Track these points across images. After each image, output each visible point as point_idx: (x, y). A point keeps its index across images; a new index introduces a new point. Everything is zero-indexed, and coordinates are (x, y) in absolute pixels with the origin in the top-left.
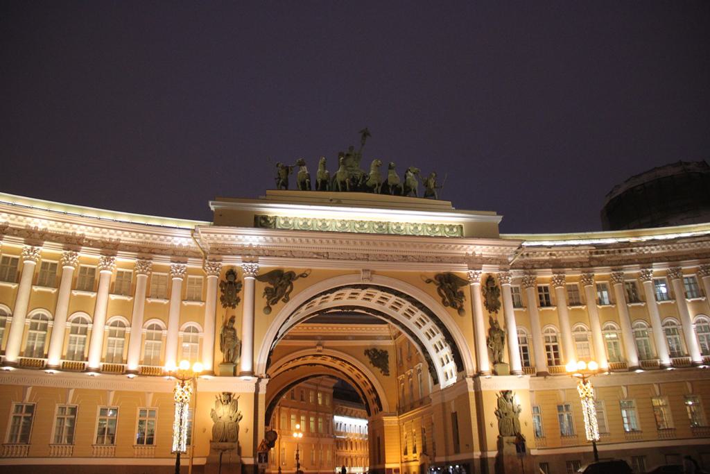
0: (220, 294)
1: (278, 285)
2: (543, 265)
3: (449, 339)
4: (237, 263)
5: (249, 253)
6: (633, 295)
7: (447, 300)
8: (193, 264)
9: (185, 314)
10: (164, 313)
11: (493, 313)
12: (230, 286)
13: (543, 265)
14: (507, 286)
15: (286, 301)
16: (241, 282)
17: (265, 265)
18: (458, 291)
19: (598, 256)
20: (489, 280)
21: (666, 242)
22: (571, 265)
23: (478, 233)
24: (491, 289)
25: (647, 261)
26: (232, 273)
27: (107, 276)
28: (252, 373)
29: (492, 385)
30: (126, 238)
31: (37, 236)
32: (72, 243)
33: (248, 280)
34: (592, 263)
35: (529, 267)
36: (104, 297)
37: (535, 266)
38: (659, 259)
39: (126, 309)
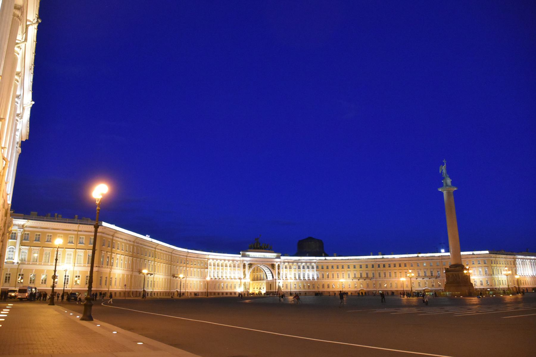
1: (250, 265)
3: (272, 273)
4: (245, 262)
5: (247, 261)
6: (299, 268)
8: (239, 262)
9: (238, 270)
10: (235, 270)
12: (244, 266)
17: (249, 262)
23: (278, 257)
24: (279, 266)
25: (302, 263)
29: (278, 281)
32: (225, 260)
35: (284, 262)
39: (231, 269)
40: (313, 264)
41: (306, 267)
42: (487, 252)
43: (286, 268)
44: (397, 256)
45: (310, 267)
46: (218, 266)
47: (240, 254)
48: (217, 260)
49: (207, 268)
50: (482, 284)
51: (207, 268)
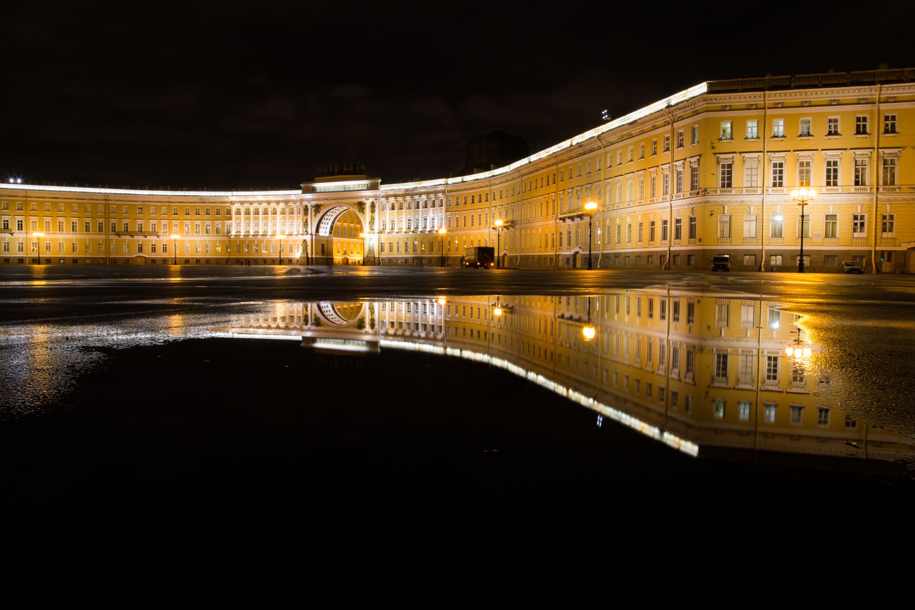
1: (317, 208)
2: (392, 196)
5: (309, 201)
13: (392, 196)
14: (377, 205)
17: (314, 203)
19: (407, 193)
20: (373, 203)
21: (426, 187)
22: (399, 196)
24: (373, 206)
25: (420, 194)
27: (279, 210)
30: (281, 199)
32: (269, 203)
35: (387, 197)
36: (279, 216)
38: (424, 193)
39: (284, 218)
40: (440, 195)
41: (430, 204)
42: (701, 88)
43: (393, 208)
44: (543, 154)
45: (437, 203)
46: (257, 212)
47: (300, 188)
48: (251, 203)
49: (230, 219)
50: (830, 234)
51: (230, 219)
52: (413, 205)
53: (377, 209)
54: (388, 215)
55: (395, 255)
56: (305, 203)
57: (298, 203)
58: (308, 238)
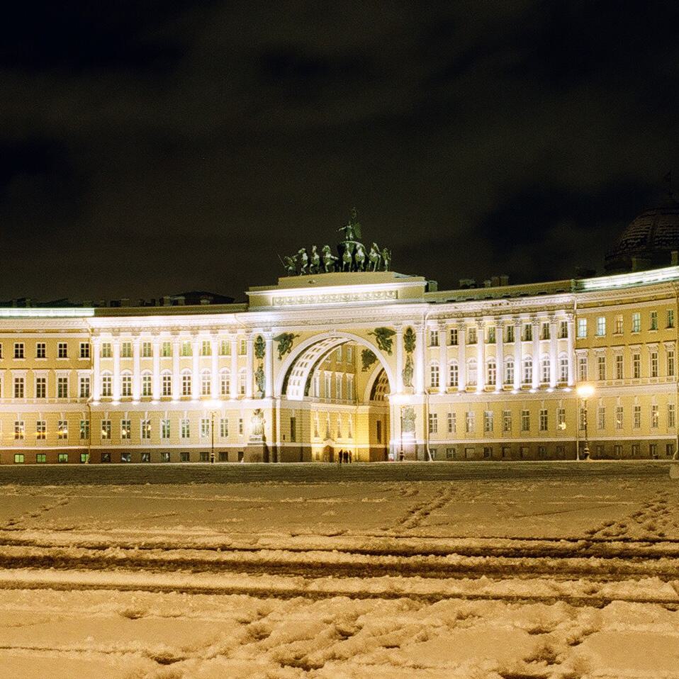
0: (255, 351)
1: (286, 341)
7: (382, 346)
11: (410, 353)
12: (260, 346)
15: (289, 352)
16: (265, 342)
18: (388, 339)
20: (409, 330)
26: (260, 338)
28: (273, 398)
31: (157, 329)
33: (268, 342)
34: (483, 313)
36: (196, 358)
37: (446, 316)
45: (555, 330)
51: (89, 366)
52: (500, 335)
53: (419, 343)
54: (443, 357)
55: (458, 439)
56: (258, 331)
57: (241, 332)
58: (266, 405)
